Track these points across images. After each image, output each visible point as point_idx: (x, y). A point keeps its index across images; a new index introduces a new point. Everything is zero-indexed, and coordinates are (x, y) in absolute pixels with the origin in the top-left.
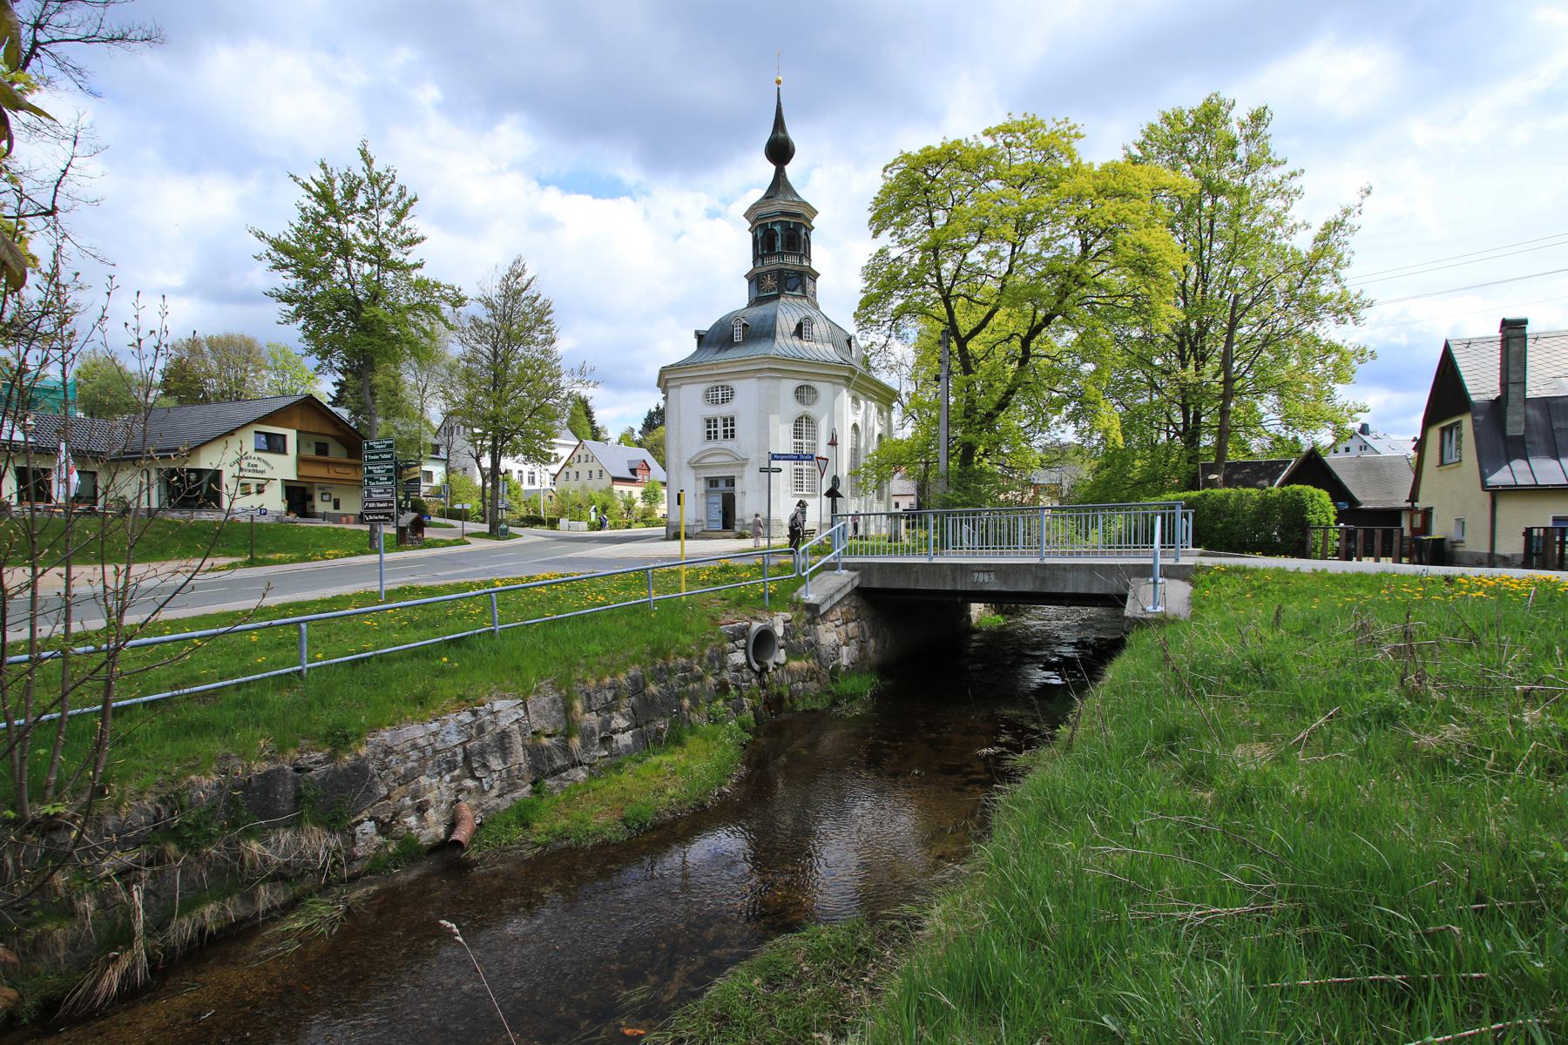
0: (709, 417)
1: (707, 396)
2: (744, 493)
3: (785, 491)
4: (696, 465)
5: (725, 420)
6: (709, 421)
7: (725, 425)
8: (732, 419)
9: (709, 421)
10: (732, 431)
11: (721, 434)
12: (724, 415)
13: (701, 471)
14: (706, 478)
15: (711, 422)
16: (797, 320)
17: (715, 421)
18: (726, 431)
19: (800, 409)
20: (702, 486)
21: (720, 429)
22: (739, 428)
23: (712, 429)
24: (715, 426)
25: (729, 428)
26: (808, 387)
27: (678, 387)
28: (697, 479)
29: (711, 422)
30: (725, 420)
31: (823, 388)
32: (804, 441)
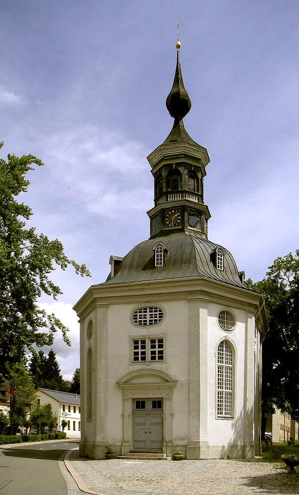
0: (136, 338)
5: (153, 341)
6: (136, 342)
7: (153, 347)
8: (161, 341)
10: (161, 352)
12: (153, 337)
15: (138, 344)
16: (210, 251)
17: (143, 342)
22: (168, 350)
24: (143, 347)
25: (157, 349)
26: (228, 313)
27: (107, 306)
29: (138, 344)
30: (153, 341)
31: (237, 313)
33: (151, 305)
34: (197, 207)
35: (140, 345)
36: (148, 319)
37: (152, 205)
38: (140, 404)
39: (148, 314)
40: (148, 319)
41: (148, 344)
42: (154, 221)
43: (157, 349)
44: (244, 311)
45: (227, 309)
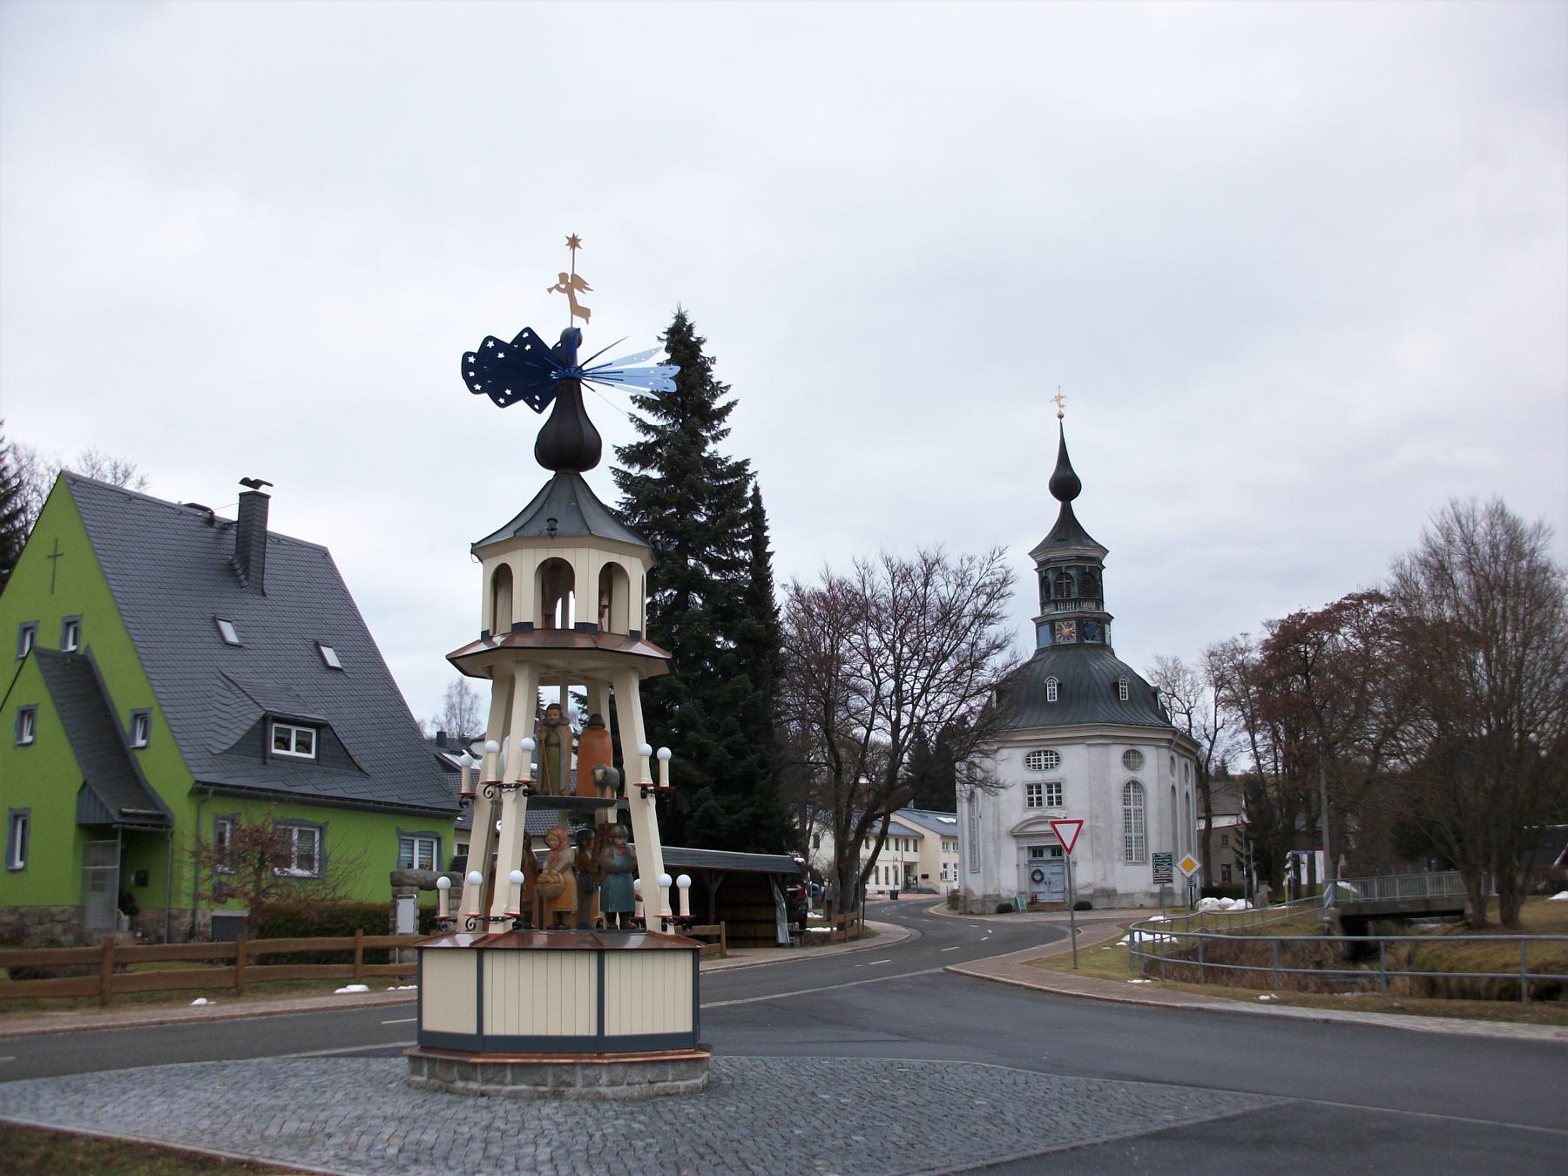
1: (1028, 761)
2: (1075, 863)
3: (1119, 860)
4: (1017, 835)
5: (1049, 786)
6: (1030, 787)
8: (1058, 785)
9: (1030, 787)
10: (1059, 798)
11: (1045, 801)
13: (1022, 840)
14: (1029, 848)
17: (1039, 786)
18: (1050, 798)
19: (1130, 775)
20: (1025, 856)
21: (1045, 795)
22: (1068, 794)
23: (1035, 796)
24: (1039, 792)
25: (1054, 795)
26: (1134, 751)
28: (1019, 849)
32: (1132, 807)
33: (1047, 749)
34: (1095, 616)
35: (1034, 790)
36: (1043, 763)
37: (1038, 613)
38: (1037, 852)
39: (1043, 757)
40: (1043, 763)
41: (1044, 789)
42: (1040, 628)
43: (1054, 795)
44: (1153, 747)
45: (1133, 748)
